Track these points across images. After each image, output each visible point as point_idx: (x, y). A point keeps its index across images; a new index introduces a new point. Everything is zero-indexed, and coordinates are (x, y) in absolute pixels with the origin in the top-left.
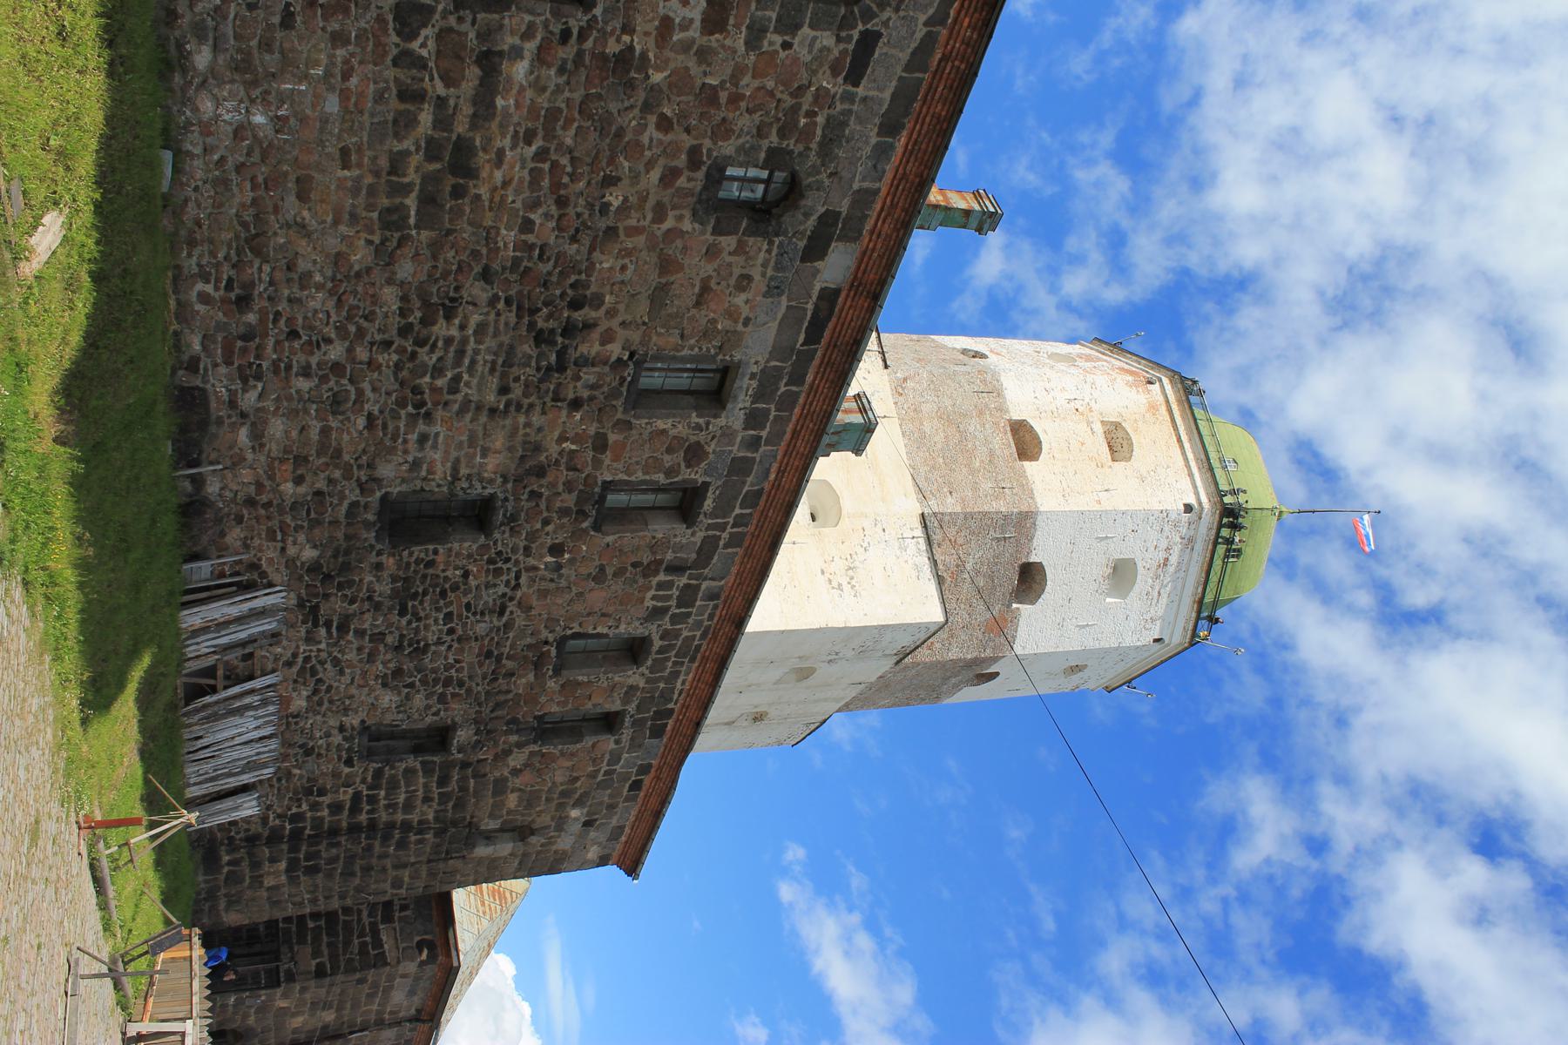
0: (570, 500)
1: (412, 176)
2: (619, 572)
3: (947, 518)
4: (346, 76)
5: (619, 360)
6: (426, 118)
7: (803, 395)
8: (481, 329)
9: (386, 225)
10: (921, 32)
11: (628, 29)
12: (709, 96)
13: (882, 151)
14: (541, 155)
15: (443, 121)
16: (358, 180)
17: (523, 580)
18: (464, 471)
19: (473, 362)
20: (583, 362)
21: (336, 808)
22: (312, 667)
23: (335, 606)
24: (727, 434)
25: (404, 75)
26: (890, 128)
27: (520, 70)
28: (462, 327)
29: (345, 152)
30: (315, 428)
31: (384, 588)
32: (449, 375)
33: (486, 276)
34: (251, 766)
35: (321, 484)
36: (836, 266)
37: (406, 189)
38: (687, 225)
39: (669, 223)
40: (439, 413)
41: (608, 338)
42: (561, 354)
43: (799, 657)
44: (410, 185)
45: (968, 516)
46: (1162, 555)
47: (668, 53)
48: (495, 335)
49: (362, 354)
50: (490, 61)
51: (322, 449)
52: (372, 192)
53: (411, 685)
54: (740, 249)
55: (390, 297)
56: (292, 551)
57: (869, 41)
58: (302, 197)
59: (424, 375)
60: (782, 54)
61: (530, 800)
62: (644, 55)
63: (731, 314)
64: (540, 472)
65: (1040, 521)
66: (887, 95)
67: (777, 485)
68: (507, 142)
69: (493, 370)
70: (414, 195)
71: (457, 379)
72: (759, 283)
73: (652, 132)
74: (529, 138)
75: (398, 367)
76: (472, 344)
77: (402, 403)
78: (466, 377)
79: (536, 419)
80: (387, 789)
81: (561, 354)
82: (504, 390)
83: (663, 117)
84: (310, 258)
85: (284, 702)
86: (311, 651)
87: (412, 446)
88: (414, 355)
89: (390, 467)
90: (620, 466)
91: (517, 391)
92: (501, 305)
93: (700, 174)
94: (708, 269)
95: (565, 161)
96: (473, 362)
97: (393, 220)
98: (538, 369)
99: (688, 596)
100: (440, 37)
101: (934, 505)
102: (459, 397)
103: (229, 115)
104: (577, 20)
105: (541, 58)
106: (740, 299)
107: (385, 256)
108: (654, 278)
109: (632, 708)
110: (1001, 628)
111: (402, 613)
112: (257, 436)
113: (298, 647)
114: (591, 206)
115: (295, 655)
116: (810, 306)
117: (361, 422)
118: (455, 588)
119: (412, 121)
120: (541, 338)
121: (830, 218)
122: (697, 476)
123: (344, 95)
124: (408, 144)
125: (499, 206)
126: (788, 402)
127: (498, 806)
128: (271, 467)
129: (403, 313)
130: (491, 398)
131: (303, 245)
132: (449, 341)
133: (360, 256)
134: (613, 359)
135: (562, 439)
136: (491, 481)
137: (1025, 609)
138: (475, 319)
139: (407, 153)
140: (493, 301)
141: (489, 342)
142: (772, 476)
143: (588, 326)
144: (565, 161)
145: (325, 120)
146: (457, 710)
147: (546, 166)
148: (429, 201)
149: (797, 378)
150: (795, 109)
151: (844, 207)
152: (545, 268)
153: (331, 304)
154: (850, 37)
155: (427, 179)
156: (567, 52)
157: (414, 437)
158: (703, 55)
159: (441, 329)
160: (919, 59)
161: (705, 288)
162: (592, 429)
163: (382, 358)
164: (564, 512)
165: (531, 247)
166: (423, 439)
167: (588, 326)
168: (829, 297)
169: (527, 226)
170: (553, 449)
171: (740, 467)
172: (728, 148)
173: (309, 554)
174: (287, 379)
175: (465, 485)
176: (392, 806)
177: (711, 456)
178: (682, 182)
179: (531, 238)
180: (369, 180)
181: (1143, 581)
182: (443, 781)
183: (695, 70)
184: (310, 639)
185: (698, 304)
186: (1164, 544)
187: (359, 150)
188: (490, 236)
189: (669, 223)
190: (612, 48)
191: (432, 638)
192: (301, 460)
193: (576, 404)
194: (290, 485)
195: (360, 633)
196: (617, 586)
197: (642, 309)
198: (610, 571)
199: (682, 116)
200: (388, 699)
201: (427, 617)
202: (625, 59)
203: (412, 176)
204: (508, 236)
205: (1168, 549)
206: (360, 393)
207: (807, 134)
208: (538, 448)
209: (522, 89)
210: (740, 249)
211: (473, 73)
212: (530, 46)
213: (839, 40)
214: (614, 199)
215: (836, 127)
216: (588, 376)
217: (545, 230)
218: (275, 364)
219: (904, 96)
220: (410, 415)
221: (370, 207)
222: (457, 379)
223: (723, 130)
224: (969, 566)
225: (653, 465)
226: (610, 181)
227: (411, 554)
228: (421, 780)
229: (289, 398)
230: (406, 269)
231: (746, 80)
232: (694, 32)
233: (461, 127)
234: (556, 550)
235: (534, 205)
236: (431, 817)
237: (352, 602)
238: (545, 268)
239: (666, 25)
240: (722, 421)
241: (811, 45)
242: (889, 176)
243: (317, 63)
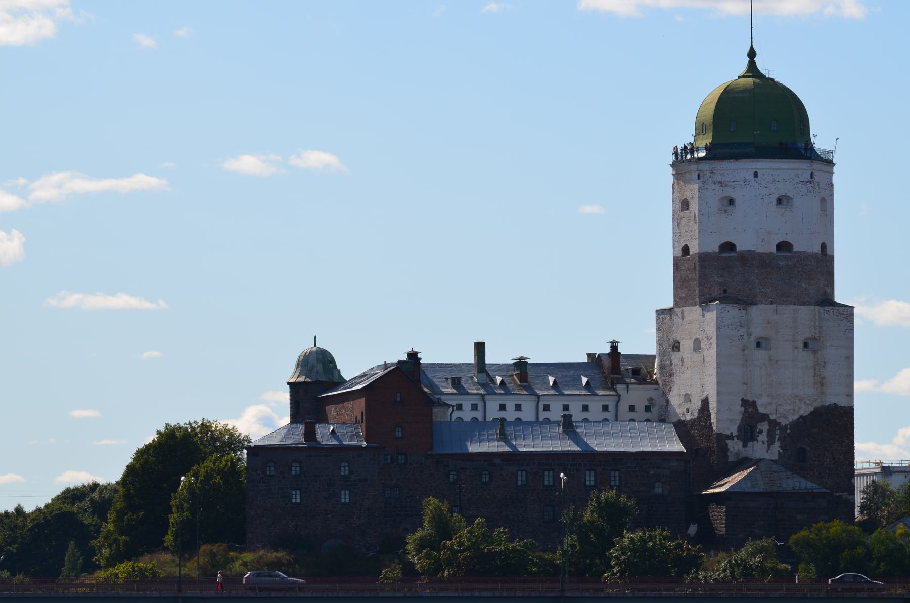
3: (701, 294)
14: (482, 508)
43: (743, 350)
45: (700, 285)
46: (717, 186)
65: (702, 252)
101: (697, 300)
110: (747, 258)
137: (738, 249)
181: (729, 192)
186: (713, 186)
205: (715, 183)
214: (488, 497)
224: (719, 280)
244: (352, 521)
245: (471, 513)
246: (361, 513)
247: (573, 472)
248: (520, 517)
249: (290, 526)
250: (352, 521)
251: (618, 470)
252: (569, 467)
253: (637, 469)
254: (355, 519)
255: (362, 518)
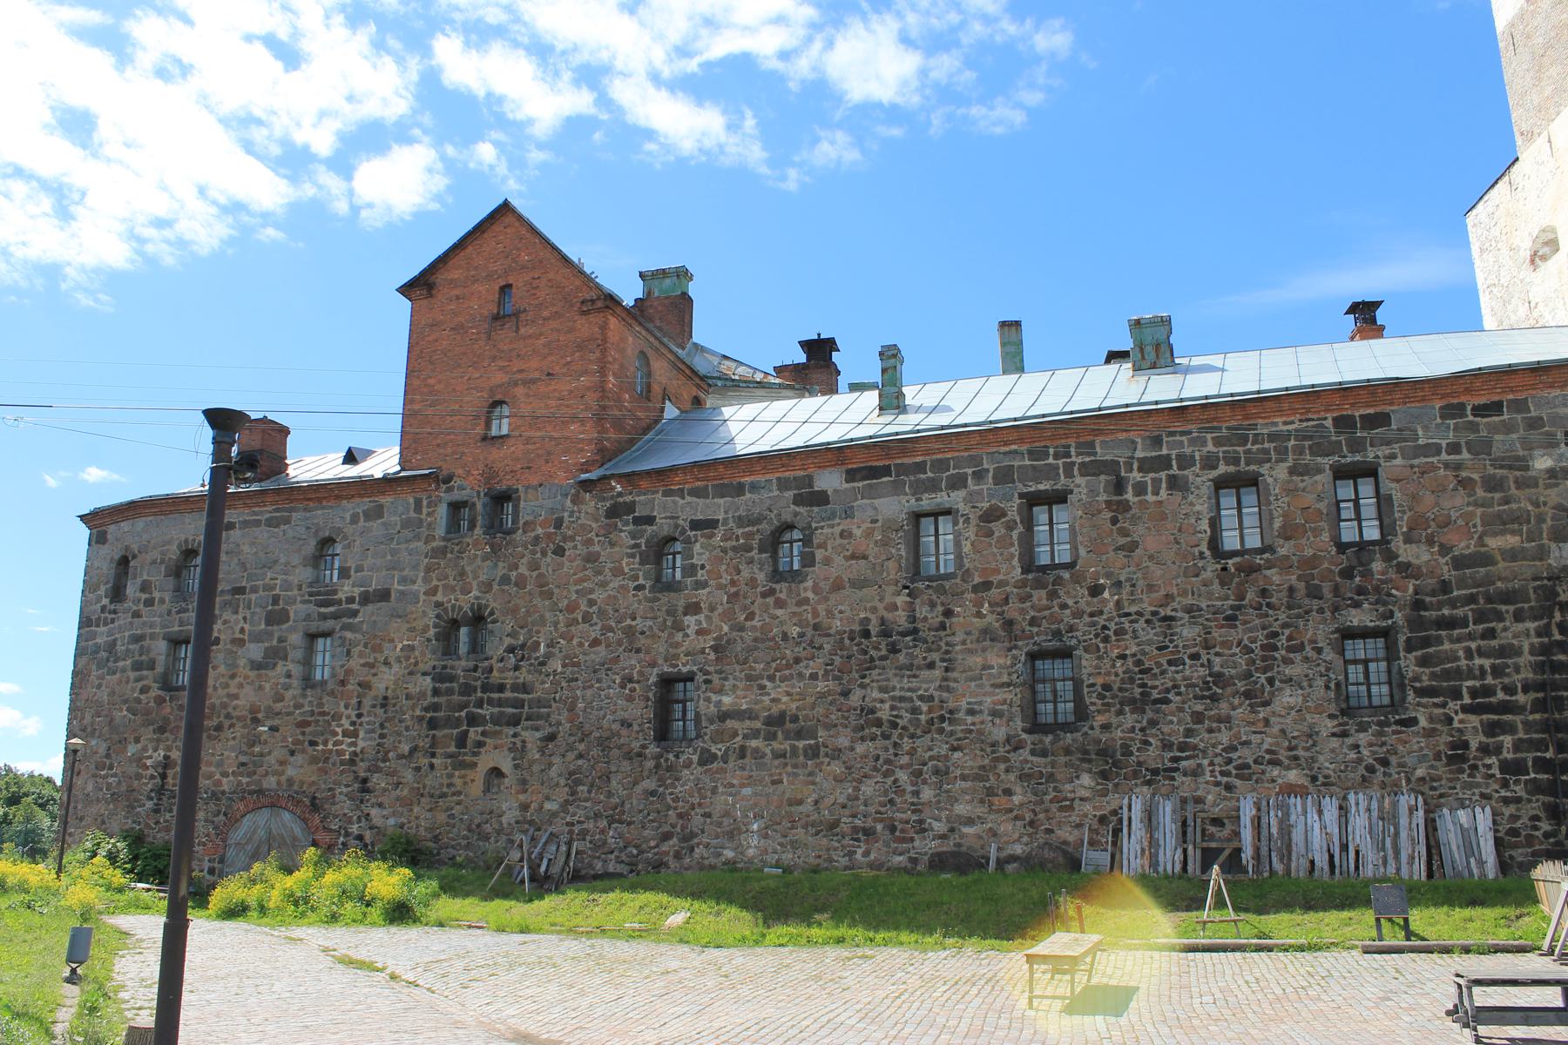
0: (1040, 596)
1: (786, 746)
2: (1124, 533)
4: (733, 786)
5: (909, 595)
6: (754, 743)
7: (935, 457)
8: (883, 690)
9: (816, 755)
10: (688, 499)
11: (703, 651)
12: (733, 597)
13: (754, 487)
14: (771, 678)
15: (755, 734)
16: (789, 775)
17: (1133, 609)
18: (1005, 679)
19: (910, 690)
20: (913, 619)
21: (1492, 729)
22: (1237, 768)
23: (1154, 755)
24: (971, 499)
25: (732, 758)
26: (739, 490)
27: (727, 700)
28: (882, 701)
29: (774, 783)
30: (960, 784)
31: (1129, 719)
32: (919, 703)
33: (846, 694)
34: (1388, 817)
35: (1012, 777)
36: (830, 480)
37: (794, 748)
38: (809, 583)
39: (810, 595)
40: (951, 705)
41: (894, 607)
42: (904, 634)
44: (791, 745)
47: (713, 627)
48: (888, 680)
49: (905, 760)
50: (724, 716)
51: (977, 778)
52: (795, 766)
53: (1271, 681)
54: (823, 546)
55: (860, 749)
56: (1086, 794)
57: (696, 525)
58: (800, 802)
59: (918, 719)
60: (708, 567)
61: (1501, 523)
62: (715, 639)
63: (869, 534)
64: (1009, 624)
66: (722, 501)
67: (1021, 441)
68: (766, 698)
69: (915, 676)
70: (797, 743)
71: (921, 698)
72: (845, 525)
73: (756, 623)
74: (762, 687)
75: (912, 736)
76: (897, 693)
77: (941, 731)
78: (920, 692)
79: (957, 639)
80: (1462, 680)
81: (904, 634)
82: (931, 666)
83: (746, 619)
84: (841, 794)
85: (1291, 790)
86: (1212, 771)
87: (977, 719)
88: (903, 728)
89: (995, 731)
90: (1005, 566)
91: (935, 656)
92: (867, 681)
93: (777, 587)
94: (839, 560)
95: (774, 665)
96: (910, 690)
97: (813, 752)
98: (916, 646)
99: (1146, 466)
100: (715, 742)
102: (936, 694)
103: (754, 841)
104: (700, 678)
105: (720, 691)
106: (857, 532)
107: (836, 754)
108: (847, 591)
109: (1326, 462)
111: (1166, 701)
112: (970, 821)
113: (1207, 783)
114: (798, 644)
115: (1217, 784)
116: (860, 484)
117: (957, 755)
118: (1138, 663)
119: (756, 750)
120: (894, 649)
121: (799, 500)
122: (1013, 508)
123: (743, 786)
124: (768, 751)
125: (802, 696)
126: (941, 465)
127: (1512, 555)
128: (998, 811)
129: (873, 739)
130: (937, 673)
131: (828, 801)
132: (893, 708)
133: (837, 768)
134: (908, 599)
135: (979, 615)
136: (1015, 657)
138: (876, 694)
139: (772, 751)
140: (863, 686)
141: (895, 682)
142: (1014, 447)
143: (883, 621)
144: (774, 665)
145: (756, 794)
146: (1319, 630)
147: (778, 674)
148: (799, 735)
149: (920, 467)
150: (734, 549)
151: (790, 494)
152: (838, 660)
153: (869, 782)
154: (695, 536)
155: (787, 738)
156: (715, 678)
157: (970, 719)
158: (712, 609)
159: (884, 713)
160: (698, 493)
161: (853, 557)
162: (969, 596)
163: (906, 747)
164: (1053, 595)
165: (826, 671)
166: (971, 712)
167: (883, 621)
168: (851, 475)
169: (814, 677)
170: (991, 618)
171: (1004, 476)
172: (761, 577)
173: (1086, 780)
174: (923, 804)
175: (1015, 676)
176: (1497, 671)
177: (993, 502)
178: (783, 596)
179: (821, 673)
180: (789, 769)
182: (1451, 623)
183: (720, 610)
184: (1196, 773)
185: (865, 557)
187: (771, 775)
188: (822, 696)
189: (810, 595)
190: (712, 656)
191: (1203, 671)
192: (990, 792)
193: (948, 613)
194: (1015, 798)
195: (1189, 733)
196: (1138, 531)
197: (871, 591)
198: (1122, 541)
199: (745, 608)
200: (1288, 698)
201: (1174, 680)
202: (715, 649)
203: (786, 746)
204: (821, 686)
206: (931, 758)
207: (749, 536)
208: (985, 631)
209: (737, 697)
210: (823, 546)
211: (730, 723)
212: (714, 698)
213: (696, 541)
214: (795, 631)
215: (741, 522)
216: (922, 611)
217: (816, 666)
218: (914, 812)
219: (722, 491)
220: (950, 724)
221: (805, 766)
222: (921, 698)
223: (752, 582)
225: (1004, 542)
226: (785, 637)
227: (1093, 704)
228: (1447, 646)
229: (939, 802)
230: (843, 742)
231: (723, 581)
232: (701, 617)
233: (758, 725)
234: (1096, 591)
235: (800, 675)
236: (1532, 625)
237: (1147, 743)
238: (838, 660)
239: (699, 632)
240: (961, 506)
241: (701, 554)
242: (768, 477)
243: (726, 800)
244: (330, 747)
245: (727, 700)
246: (359, 716)
247: (1156, 493)
248: (925, 708)
249: (149, 762)
250: (330, 747)
251: (1371, 471)
252: (1136, 476)
253: (1465, 455)
254: (340, 737)
255: (362, 734)
